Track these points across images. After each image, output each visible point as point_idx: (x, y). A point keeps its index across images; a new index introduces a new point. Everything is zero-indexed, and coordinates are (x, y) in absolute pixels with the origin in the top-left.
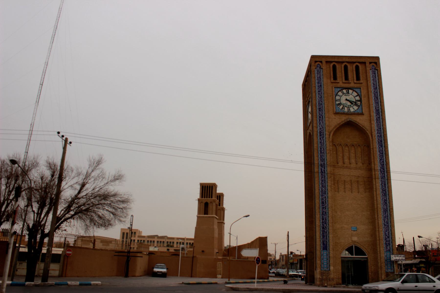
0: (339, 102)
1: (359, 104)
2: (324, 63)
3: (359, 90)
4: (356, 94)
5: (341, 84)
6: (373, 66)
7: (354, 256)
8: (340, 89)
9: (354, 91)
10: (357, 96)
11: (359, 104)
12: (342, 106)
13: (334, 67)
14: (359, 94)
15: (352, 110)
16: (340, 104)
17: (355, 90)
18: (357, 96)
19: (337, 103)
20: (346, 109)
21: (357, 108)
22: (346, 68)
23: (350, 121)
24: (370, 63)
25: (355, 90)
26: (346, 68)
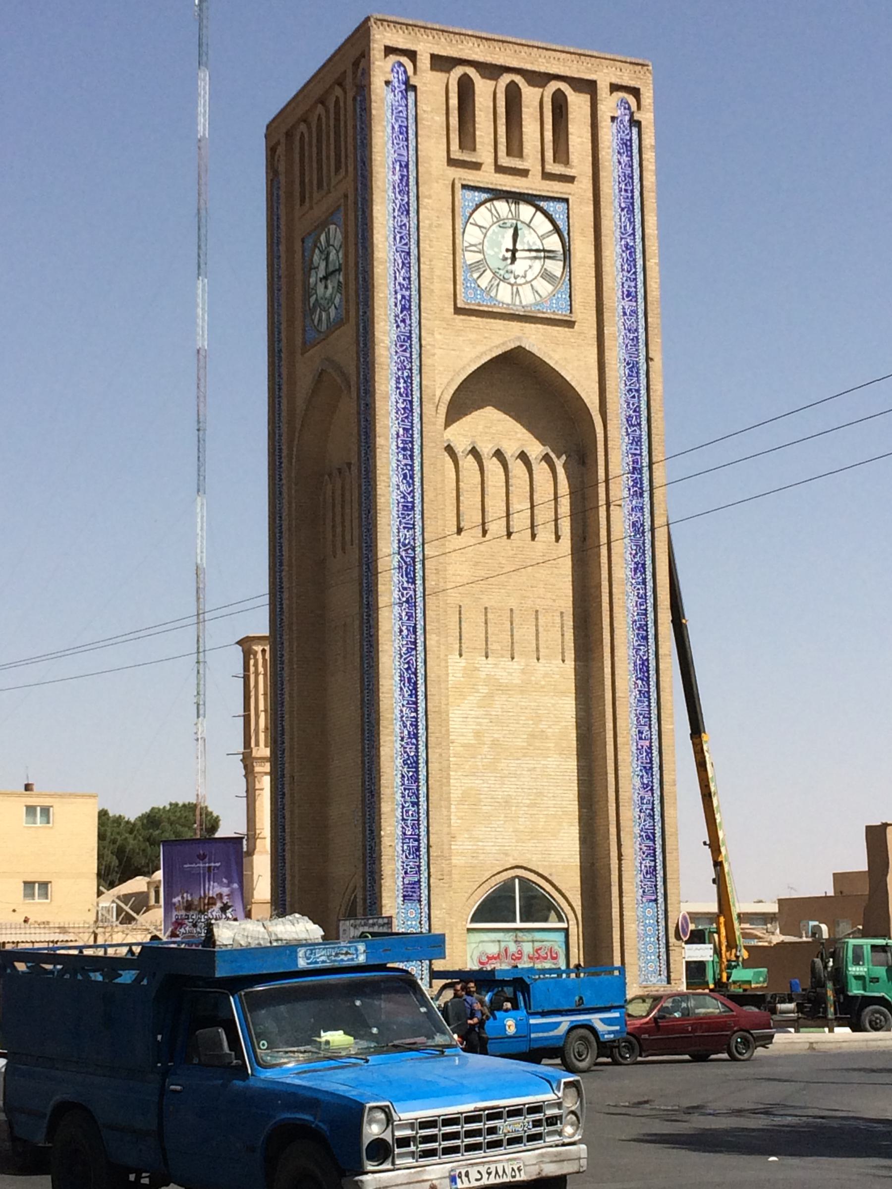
0: (480, 257)
1: (558, 273)
2: (424, 61)
3: (561, 206)
4: (550, 227)
5: (488, 177)
6: (624, 102)
7: (518, 925)
8: (485, 196)
9: (539, 208)
10: (548, 235)
11: (558, 273)
12: (488, 275)
13: (466, 88)
14: (562, 225)
15: (527, 298)
16: (480, 266)
17: (542, 204)
18: (548, 235)
19: (471, 258)
20: (504, 294)
21: (550, 288)
22: (513, 97)
23: (520, 347)
24: (615, 88)
25: (542, 204)
26: (513, 97)
